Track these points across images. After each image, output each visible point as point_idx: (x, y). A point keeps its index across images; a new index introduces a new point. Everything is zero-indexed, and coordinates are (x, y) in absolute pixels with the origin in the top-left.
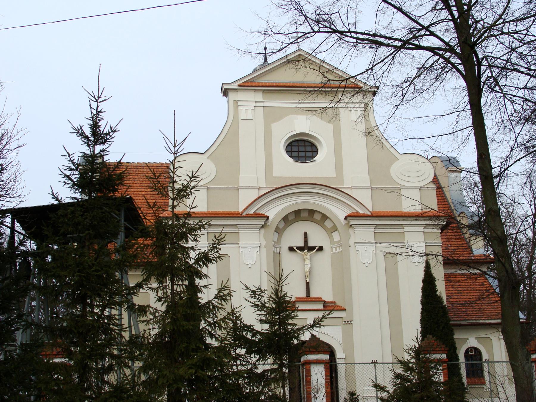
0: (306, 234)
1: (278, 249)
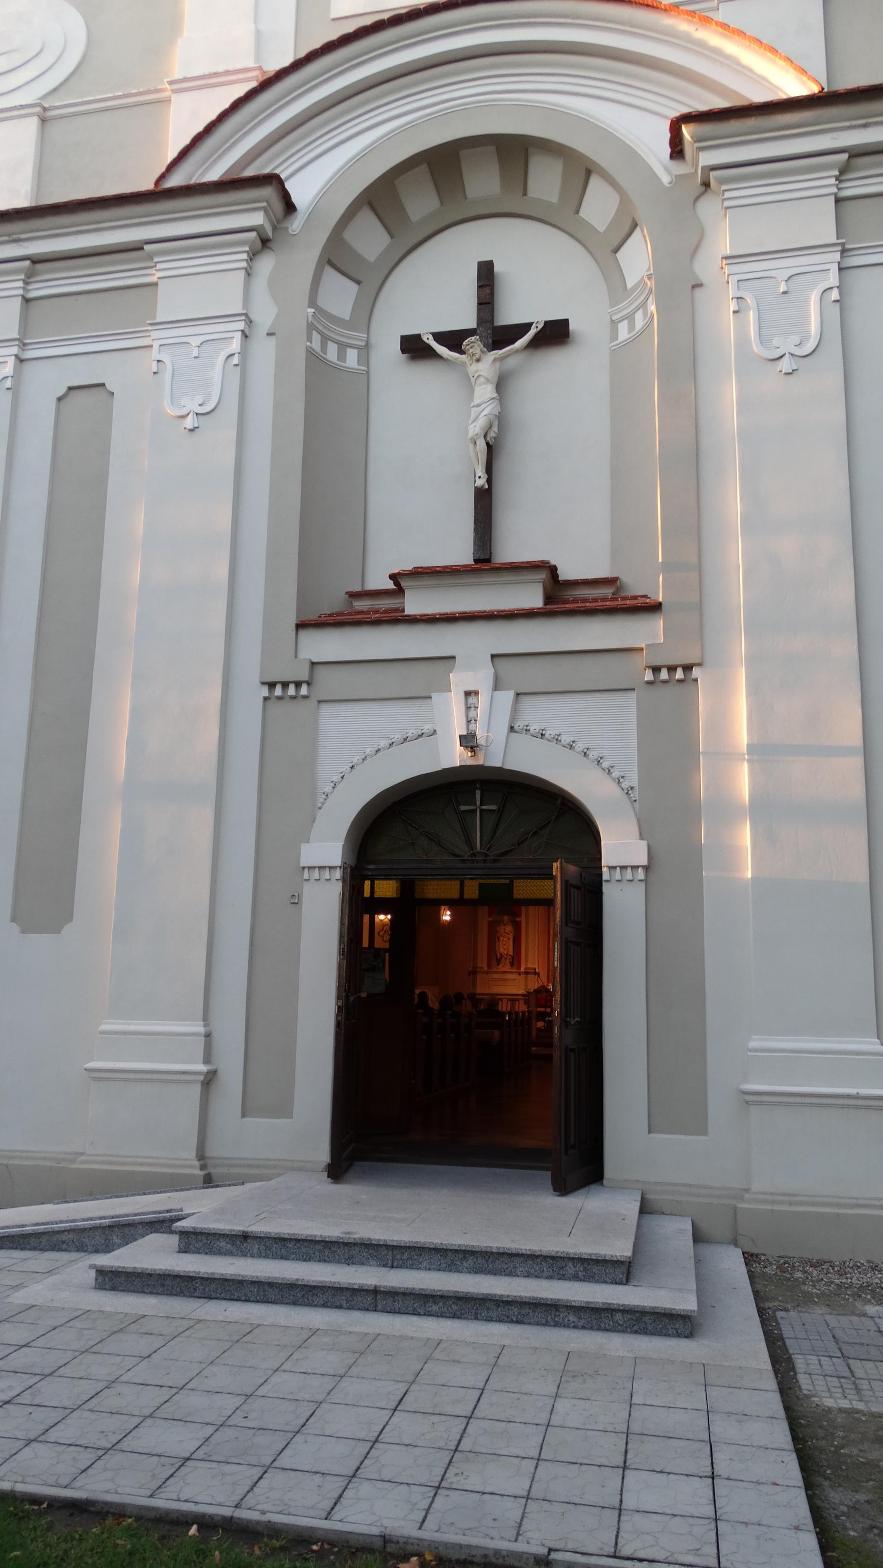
0: (486, 274)
1: (352, 357)
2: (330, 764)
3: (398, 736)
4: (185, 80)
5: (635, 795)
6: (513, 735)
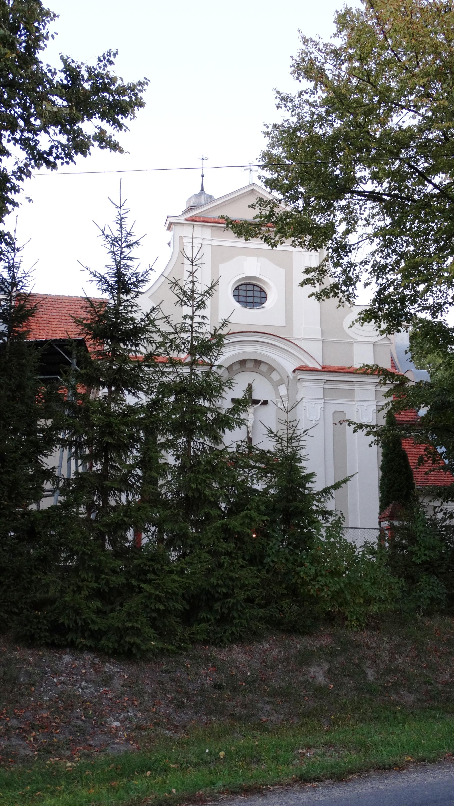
0: (250, 386)
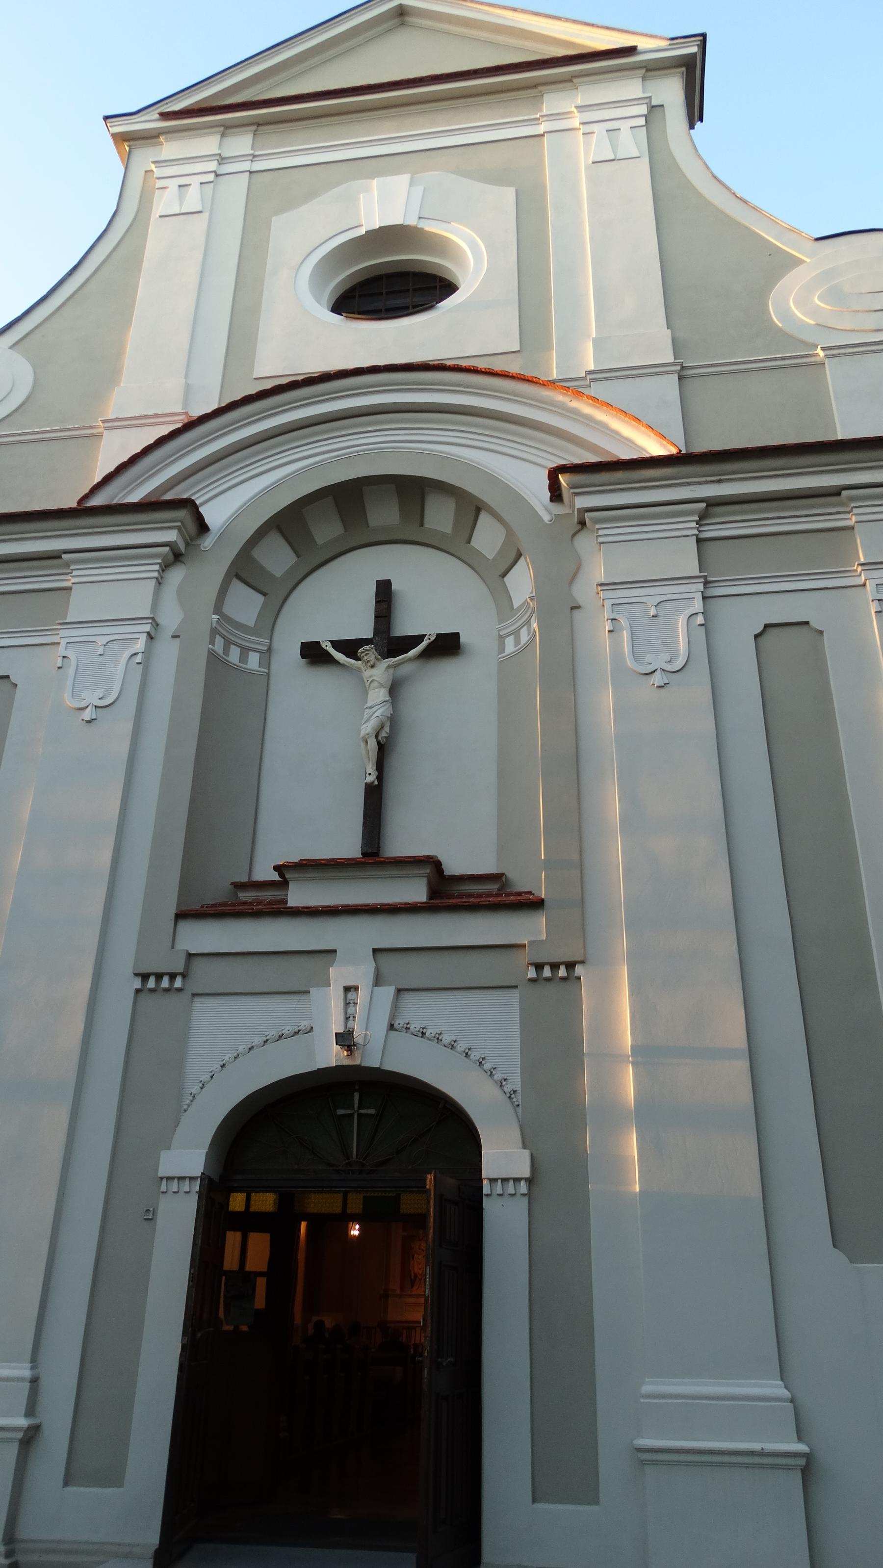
0: (384, 593)
1: (253, 661)
2: (201, 1061)
3: (273, 1033)
4: (118, 419)
5: (518, 1099)
6: (393, 1034)
